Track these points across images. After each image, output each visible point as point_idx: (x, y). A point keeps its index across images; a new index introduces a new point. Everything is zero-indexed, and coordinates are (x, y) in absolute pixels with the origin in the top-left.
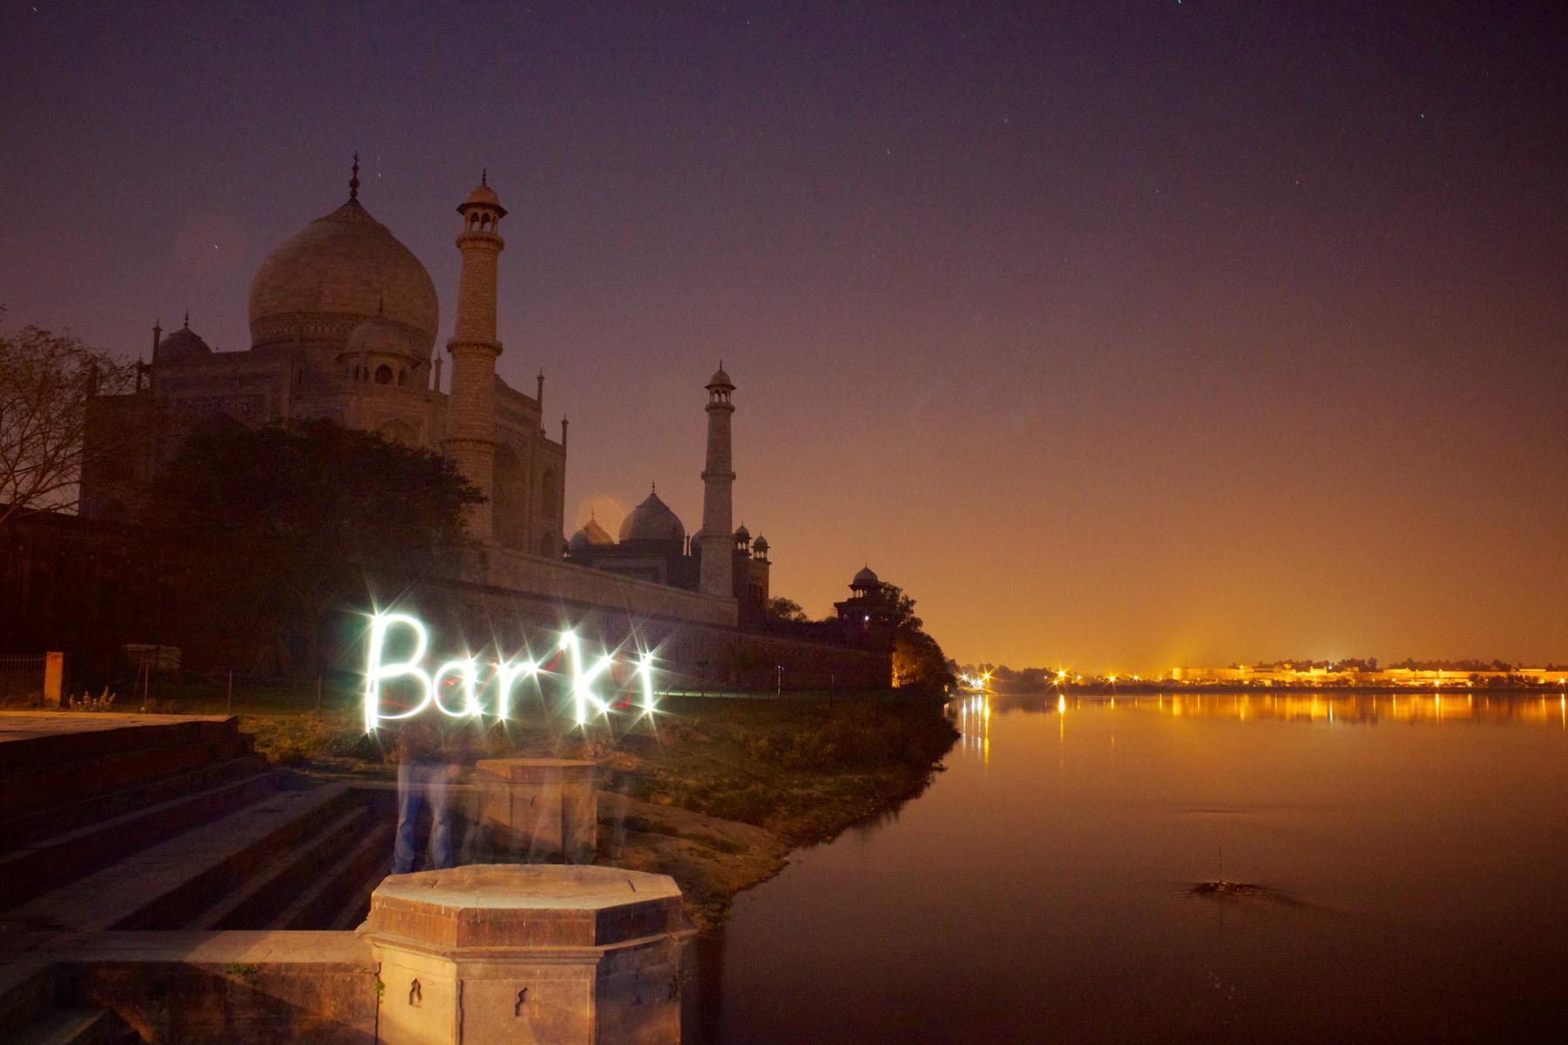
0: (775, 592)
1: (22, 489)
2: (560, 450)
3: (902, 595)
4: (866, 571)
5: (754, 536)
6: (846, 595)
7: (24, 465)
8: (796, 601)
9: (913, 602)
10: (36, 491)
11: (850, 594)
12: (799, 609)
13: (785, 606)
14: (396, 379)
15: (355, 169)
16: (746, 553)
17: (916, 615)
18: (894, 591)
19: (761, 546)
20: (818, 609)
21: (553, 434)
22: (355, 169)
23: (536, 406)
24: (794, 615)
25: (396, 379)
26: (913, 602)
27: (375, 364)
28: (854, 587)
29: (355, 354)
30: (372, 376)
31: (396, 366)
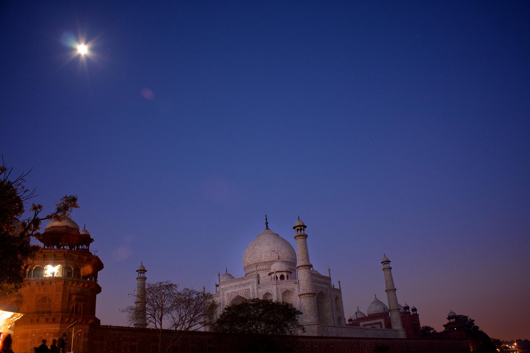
0: (423, 324)
1: (186, 327)
2: (339, 291)
3: (469, 318)
4: (452, 312)
5: (411, 308)
6: (446, 322)
7: (186, 321)
8: (431, 326)
9: (473, 321)
10: (190, 327)
11: (448, 321)
12: (433, 329)
13: (427, 328)
14: (286, 278)
15: (266, 219)
16: (409, 313)
17: (476, 325)
18: (465, 318)
19: (414, 310)
20: (439, 328)
21: (337, 287)
22: (266, 219)
23: (329, 279)
24: (432, 331)
25: (286, 278)
26: (473, 321)
27: (278, 275)
28: (449, 318)
29: (273, 273)
30: (279, 278)
31: (285, 274)
